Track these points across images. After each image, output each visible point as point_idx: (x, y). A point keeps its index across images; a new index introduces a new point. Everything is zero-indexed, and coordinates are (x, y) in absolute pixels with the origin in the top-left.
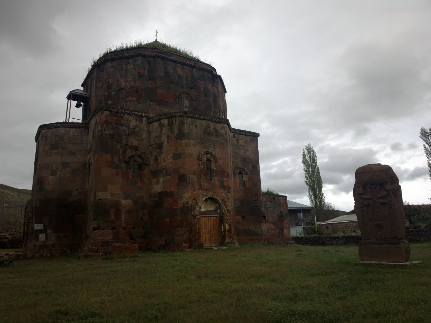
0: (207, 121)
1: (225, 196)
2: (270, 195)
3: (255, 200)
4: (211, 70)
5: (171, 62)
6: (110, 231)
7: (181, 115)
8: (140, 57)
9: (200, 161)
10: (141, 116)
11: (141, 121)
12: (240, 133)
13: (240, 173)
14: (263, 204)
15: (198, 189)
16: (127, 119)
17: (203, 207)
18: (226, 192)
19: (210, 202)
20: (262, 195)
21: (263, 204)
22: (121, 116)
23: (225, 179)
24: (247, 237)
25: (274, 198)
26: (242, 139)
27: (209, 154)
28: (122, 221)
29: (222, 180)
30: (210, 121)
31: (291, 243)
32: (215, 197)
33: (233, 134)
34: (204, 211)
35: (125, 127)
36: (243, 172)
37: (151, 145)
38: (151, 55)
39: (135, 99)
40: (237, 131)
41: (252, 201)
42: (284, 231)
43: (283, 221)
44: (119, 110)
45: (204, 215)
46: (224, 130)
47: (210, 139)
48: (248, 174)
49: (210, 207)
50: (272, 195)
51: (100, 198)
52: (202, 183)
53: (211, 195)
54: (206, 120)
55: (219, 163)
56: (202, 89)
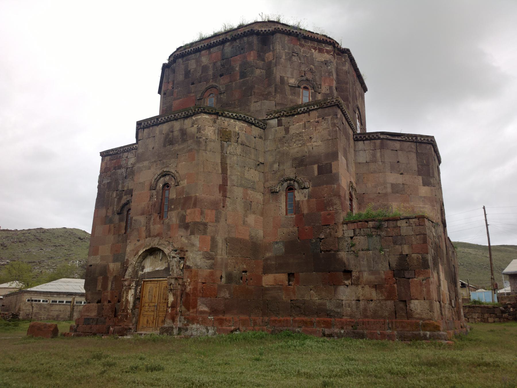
0: (169, 123)
1: (187, 241)
2: (367, 222)
3: (323, 237)
4: (252, 30)
5: (193, 55)
6: (95, 304)
9: (154, 191)
12: (289, 114)
13: (290, 189)
14: (345, 244)
15: (145, 237)
18: (189, 234)
20: (343, 223)
21: (345, 244)
23: (189, 211)
24: (297, 318)
25: (379, 228)
26: (298, 123)
27: (169, 175)
29: (184, 213)
30: (175, 121)
31: (428, 336)
32: (159, 247)
33: (276, 120)
34: (148, 273)
36: (296, 185)
40: (285, 111)
41: (314, 241)
42: (412, 306)
43: (409, 278)
45: (149, 279)
47: (172, 149)
48: (304, 188)
49: (159, 265)
50: (373, 220)
51: (90, 264)
52: (152, 226)
53: (156, 244)
54: (167, 121)
55: (181, 186)
56: (237, 69)
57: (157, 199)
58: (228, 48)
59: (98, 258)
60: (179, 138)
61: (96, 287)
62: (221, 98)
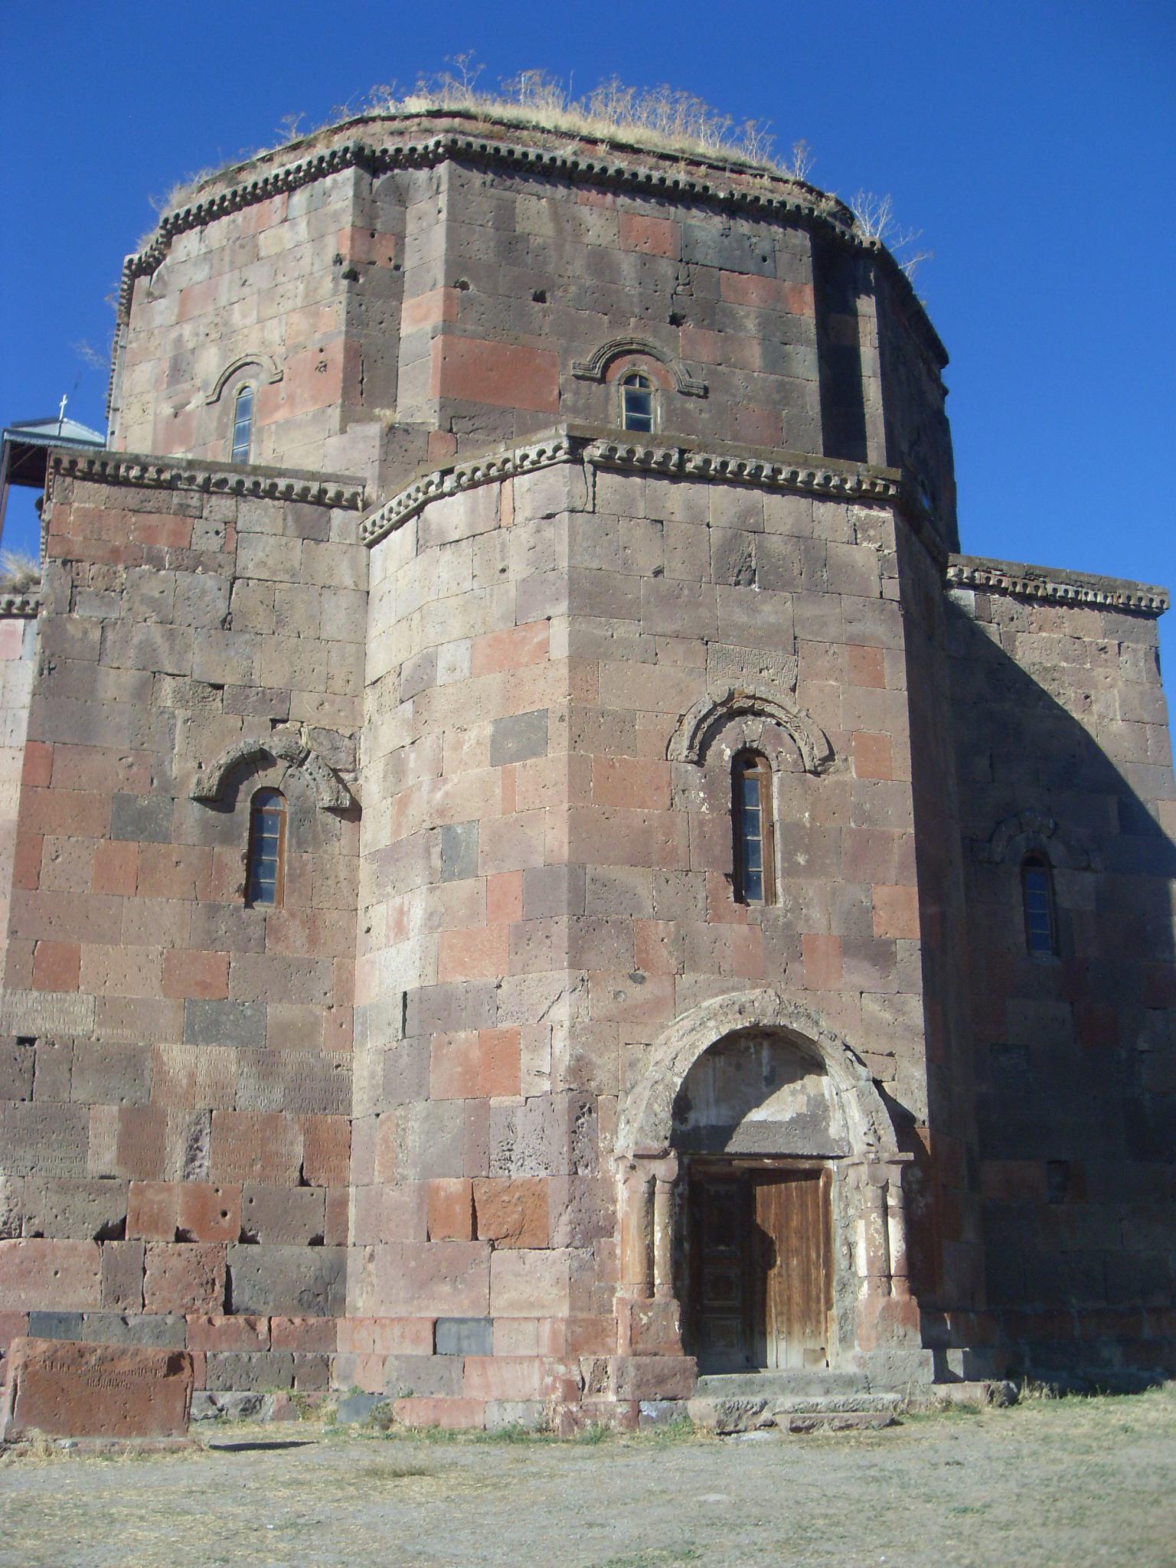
1: (887, 1016)
7: (549, 453)
8: (349, 173)
10: (319, 500)
11: (314, 535)
16: (225, 523)
17: (712, 1096)
19: (765, 1054)
22: (183, 508)
27: (759, 714)
28: (169, 1189)
33: (972, 593)
35: (205, 572)
36: (1056, 851)
37: (374, 680)
38: (413, 150)
39: (306, 411)
44: (174, 473)
46: (874, 546)
53: (770, 1010)
54: (736, 481)
56: (751, 325)
57: (711, 809)
58: (706, 226)
59: (81, 1010)
60: (796, 572)
61: (83, 1159)
62: (686, 412)
